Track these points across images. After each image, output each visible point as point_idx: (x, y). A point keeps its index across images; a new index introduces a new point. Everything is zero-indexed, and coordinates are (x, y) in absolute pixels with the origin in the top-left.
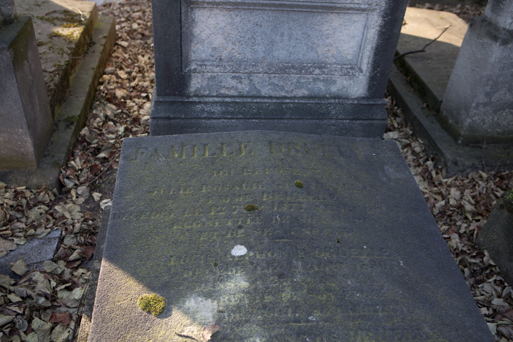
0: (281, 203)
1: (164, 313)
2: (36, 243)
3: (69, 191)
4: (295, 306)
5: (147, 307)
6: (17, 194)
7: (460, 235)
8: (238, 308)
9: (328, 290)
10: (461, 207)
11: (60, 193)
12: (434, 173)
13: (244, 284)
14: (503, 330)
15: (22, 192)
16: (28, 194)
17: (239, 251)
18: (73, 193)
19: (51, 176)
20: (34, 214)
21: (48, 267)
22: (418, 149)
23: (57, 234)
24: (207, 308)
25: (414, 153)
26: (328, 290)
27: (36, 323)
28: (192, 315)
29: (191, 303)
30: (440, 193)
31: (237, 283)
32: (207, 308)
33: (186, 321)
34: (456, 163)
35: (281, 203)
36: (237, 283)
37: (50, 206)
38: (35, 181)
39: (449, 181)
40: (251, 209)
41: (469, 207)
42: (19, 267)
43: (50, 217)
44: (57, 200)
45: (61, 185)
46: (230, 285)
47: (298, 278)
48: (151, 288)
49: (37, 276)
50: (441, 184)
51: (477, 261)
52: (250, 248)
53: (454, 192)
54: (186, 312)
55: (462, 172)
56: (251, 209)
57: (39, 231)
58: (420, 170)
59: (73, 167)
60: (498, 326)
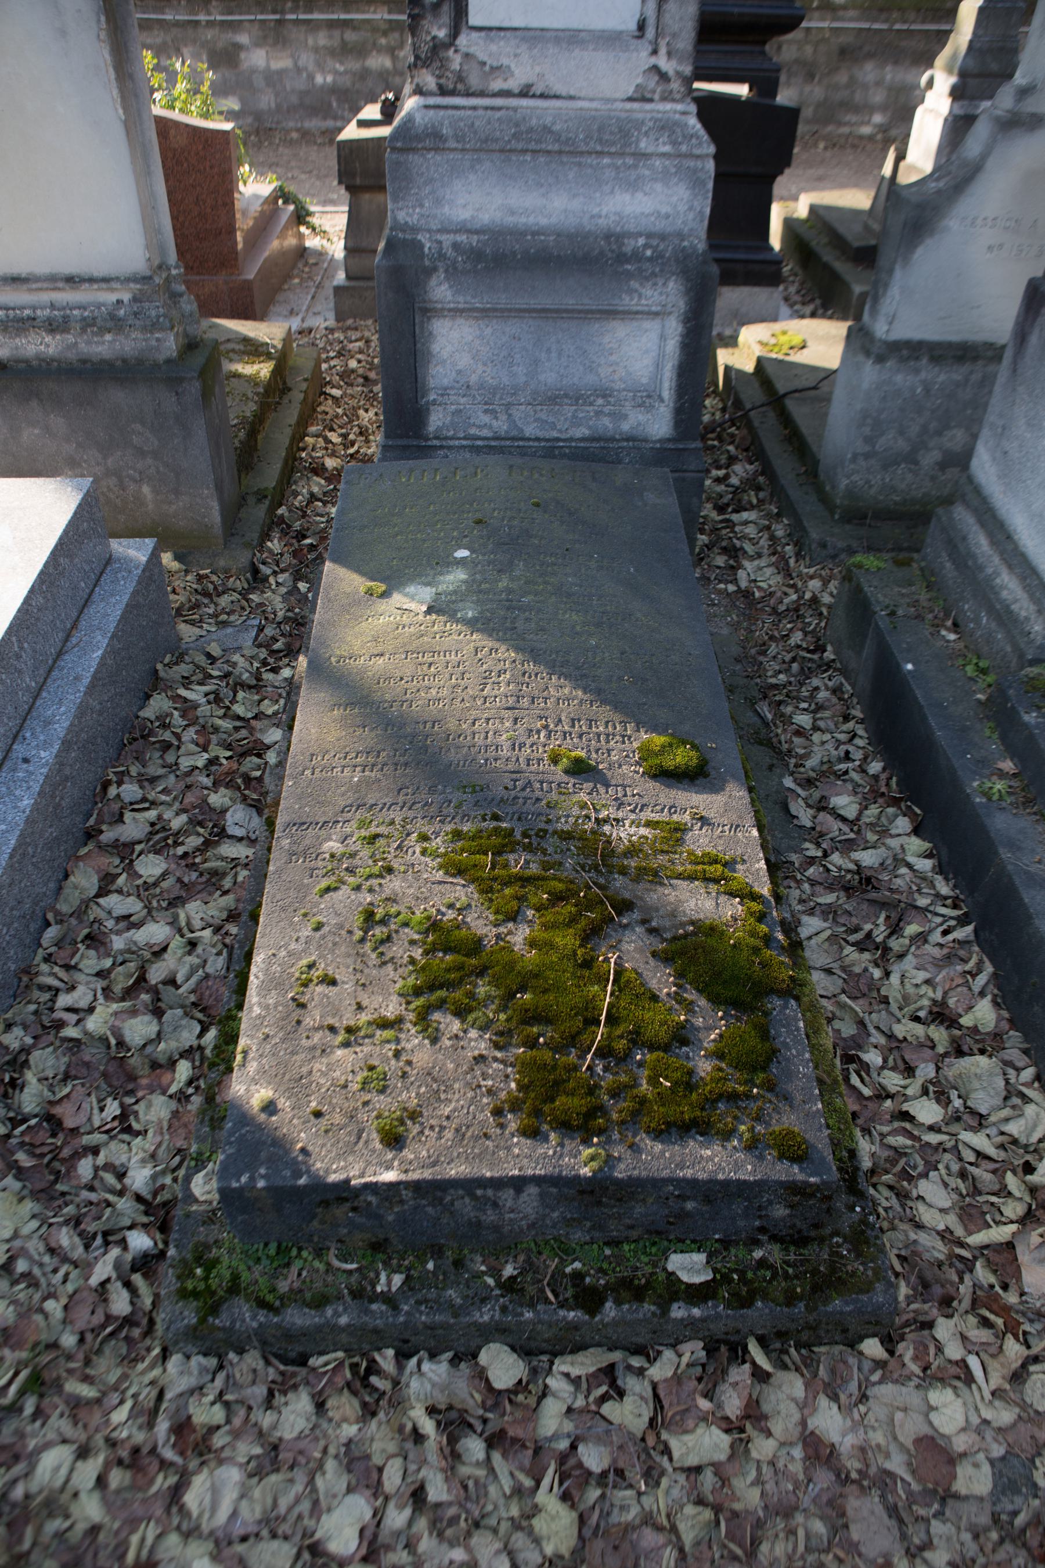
0: (512, 518)
1: (384, 595)
2: (229, 630)
3: (266, 579)
4: (509, 591)
5: (370, 592)
6: (200, 578)
7: (806, 634)
8: (455, 592)
9: (546, 583)
10: (815, 600)
11: (255, 579)
12: (792, 561)
13: (463, 576)
14: (821, 724)
15: (207, 576)
16: (214, 578)
17: (462, 553)
18: (272, 580)
19: (243, 558)
20: (224, 601)
21: (247, 652)
22: (780, 533)
23: (256, 622)
24: (427, 593)
25: (772, 538)
26: (546, 583)
27: (241, 695)
28: (412, 598)
29: (411, 589)
30: (794, 586)
31: (456, 577)
32: (427, 593)
33: (405, 600)
34: (824, 545)
35: (512, 518)
36: (456, 577)
37: (244, 594)
38: (222, 563)
39: (812, 570)
40: (479, 522)
41: (827, 599)
42: (215, 650)
43: (244, 603)
44: (252, 589)
45: (256, 571)
46: (450, 577)
47: (517, 573)
48: (373, 579)
49: (236, 658)
50: (800, 575)
51: (815, 657)
52: (472, 551)
53: (815, 584)
54: (406, 595)
55: (834, 557)
56: (479, 522)
57: (232, 618)
58: (774, 559)
59: (270, 551)
60: (815, 720)
